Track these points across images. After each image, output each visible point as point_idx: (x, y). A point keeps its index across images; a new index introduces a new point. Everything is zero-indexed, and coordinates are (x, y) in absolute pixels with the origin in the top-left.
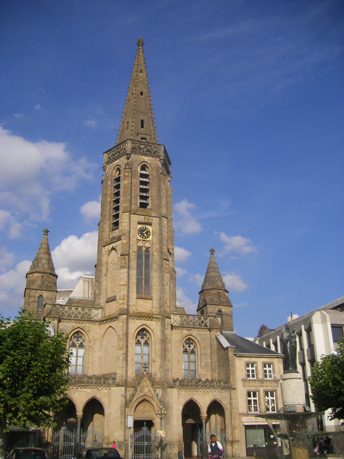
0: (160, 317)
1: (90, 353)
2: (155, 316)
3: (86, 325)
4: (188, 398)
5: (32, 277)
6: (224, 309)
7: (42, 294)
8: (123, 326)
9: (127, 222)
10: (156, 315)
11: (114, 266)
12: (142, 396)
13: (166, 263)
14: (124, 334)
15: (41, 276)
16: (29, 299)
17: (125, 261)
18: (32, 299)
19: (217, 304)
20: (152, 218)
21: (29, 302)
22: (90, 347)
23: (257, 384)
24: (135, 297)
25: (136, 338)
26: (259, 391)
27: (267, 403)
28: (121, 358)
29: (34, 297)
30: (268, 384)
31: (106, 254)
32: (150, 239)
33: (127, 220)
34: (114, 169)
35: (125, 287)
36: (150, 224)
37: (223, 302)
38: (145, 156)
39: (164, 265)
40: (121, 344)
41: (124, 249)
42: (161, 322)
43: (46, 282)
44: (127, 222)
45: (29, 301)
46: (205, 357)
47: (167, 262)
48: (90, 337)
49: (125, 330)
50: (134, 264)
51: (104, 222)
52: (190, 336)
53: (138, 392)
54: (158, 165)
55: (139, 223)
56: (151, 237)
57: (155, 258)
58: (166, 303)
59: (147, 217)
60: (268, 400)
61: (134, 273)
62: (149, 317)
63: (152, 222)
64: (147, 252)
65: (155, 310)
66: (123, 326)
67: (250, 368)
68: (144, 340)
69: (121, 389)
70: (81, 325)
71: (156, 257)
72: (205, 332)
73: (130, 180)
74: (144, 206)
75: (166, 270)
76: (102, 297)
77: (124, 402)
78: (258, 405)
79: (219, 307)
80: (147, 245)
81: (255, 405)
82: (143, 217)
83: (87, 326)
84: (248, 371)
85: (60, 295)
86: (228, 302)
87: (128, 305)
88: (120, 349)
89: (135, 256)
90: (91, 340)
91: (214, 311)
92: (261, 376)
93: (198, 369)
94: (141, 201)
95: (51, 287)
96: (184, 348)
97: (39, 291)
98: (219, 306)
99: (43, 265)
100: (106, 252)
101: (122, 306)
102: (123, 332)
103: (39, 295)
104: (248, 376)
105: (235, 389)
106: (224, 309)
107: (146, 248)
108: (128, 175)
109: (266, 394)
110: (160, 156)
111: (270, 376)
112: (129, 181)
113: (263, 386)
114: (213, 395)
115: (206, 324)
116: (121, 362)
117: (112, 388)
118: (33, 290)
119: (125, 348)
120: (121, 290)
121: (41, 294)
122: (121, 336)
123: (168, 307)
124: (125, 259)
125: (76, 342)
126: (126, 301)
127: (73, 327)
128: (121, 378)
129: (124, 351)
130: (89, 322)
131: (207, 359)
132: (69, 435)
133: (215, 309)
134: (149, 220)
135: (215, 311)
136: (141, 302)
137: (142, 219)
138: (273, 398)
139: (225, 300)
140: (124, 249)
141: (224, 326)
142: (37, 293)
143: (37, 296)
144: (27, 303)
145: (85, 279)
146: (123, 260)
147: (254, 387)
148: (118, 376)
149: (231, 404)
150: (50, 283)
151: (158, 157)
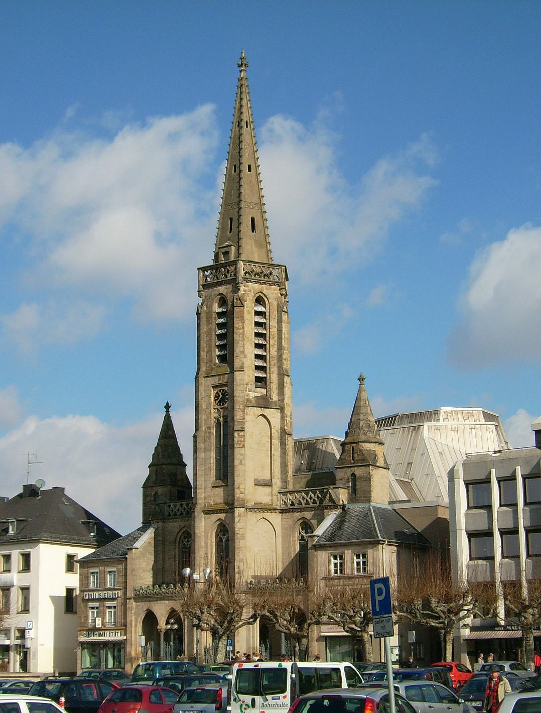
6: (358, 472)
13: (239, 435)
15: (155, 469)
37: (358, 460)
39: (236, 440)
47: (242, 433)
58: (239, 488)
75: (240, 444)
82: (218, 377)
86: (364, 460)
106: (358, 472)
133: (346, 473)
141: (358, 496)
143: (153, 493)
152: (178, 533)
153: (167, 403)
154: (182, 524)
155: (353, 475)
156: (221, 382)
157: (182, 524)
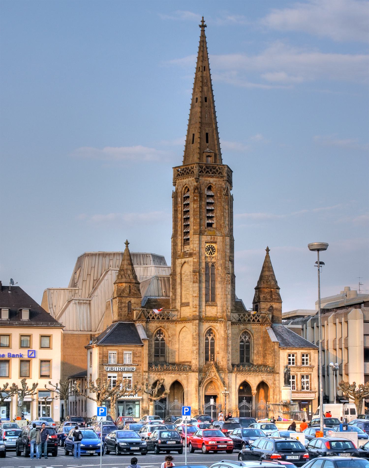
0: (223, 320)
1: (170, 346)
2: (219, 320)
3: (166, 324)
4: (243, 380)
5: (122, 286)
6: (275, 305)
7: (131, 300)
8: (196, 329)
9: (197, 244)
10: (220, 318)
11: (186, 278)
12: (210, 379)
13: (228, 276)
14: (197, 335)
15: (129, 286)
16: (121, 305)
17: (196, 277)
18: (123, 305)
19: (270, 301)
20: (217, 237)
21: (121, 308)
22: (170, 341)
23: (295, 369)
24: (205, 305)
25: (206, 336)
26: (297, 375)
27: (303, 384)
28: (195, 352)
29: (124, 303)
30: (304, 369)
31: (180, 266)
32: (215, 255)
33: (197, 242)
34: (183, 187)
35: (197, 298)
36: (215, 243)
38: (211, 178)
40: (195, 342)
41: (195, 267)
42: (224, 324)
43: (133, 290)
44: (197, 244)
45: (121, 306)
46: (257, 346)
48: (170, 333)
49: (197, 332)
50: (203, 278)
51: (176, 236)
52: (246, 330)
53: (207, 376)
54: (222, 185)
55: (206, 242)
56: (216, 254)
57: (219, 272)
58: (228, 309)
59: (213, 237)
60: (304, 381)
61: (204, 285)
62: (215, 320)
63: (217, 241)
64: (213, 266)
65: (219, 315)
66: (196, 329)
67: (291, 358)
68: (211, 337)
69: (196, 374)
70: (163, 325)
71: (220, 271)
72: (258, 326)
73: (199, 205)
74: (210, 225)
76: (177, 301)
77: (198, 383)
78: (295, 385)
79: (271, 303)
80: (213, 260)
81: (294, 385)
82: (210, 237)
83: (166, 325)
84: (290, 360)
85: (110, 259)
86: (279, 299)
87: (200, 312)
88: (194, 345)
89: (203, 271)
90: (170, 336)
91: (266, 307)
92: (299, 364)
93: (251, 355)
94: (208, 222)
95: (137, 294)
96: (241, 339)
97: (128, 298)
98: (271, 303)
99: (129, 275)
100: (180, 264)
101: (195, 313)
102: (196, 333)
103: (128, 301)
104: (290, 363)
105: (278, 373)
106: (275, 305)
107: (212, 263)
108: (197, 199)
109: (303, 377)
110: (224, 176)
111: (307, 363)
112: (198, 206)
113: (300, 371)
114: (262, 377)
115: (258, 320)
116: (195, 355)
117: (189, 373)
118: (124, 298)
119: (198, 345)
120: (194, 300)
121: (129, 300)
122: (195, 336)
123: (229, 312)
124: (195, 275)
125: (159, 338)
126: (198, 309)
127: (156, 326)
128: (195, 366)
129: (197, 347)
130: (168, 322)
131: (258, 348)
132: (161, 406)
133: (267, 305)
134: (215, 239)
135: (267, 307)
136: (208, 308)
137: (208, 238)
138: (307, 380)
139: (276, 298)
140: (195, 267)
141: (274, 319)
142: (126, 299)
143: (127, 302)
144: (120, 308)
145: (158, 278)
146: (195, 276)
147: (294, 371)
148: (193, 365)
149: (274, 384)
150: (136, 291)
151: (222, 177)
152: (154, 332)
153: (127, 241)
154: (158, 325)
155: (271, 306)
156: (212, 240)
157: (158, 325)
